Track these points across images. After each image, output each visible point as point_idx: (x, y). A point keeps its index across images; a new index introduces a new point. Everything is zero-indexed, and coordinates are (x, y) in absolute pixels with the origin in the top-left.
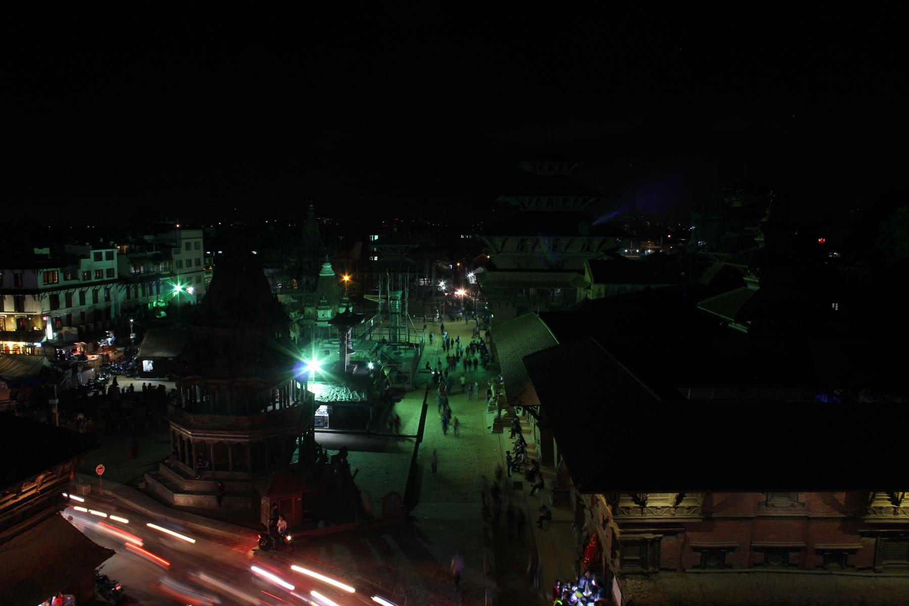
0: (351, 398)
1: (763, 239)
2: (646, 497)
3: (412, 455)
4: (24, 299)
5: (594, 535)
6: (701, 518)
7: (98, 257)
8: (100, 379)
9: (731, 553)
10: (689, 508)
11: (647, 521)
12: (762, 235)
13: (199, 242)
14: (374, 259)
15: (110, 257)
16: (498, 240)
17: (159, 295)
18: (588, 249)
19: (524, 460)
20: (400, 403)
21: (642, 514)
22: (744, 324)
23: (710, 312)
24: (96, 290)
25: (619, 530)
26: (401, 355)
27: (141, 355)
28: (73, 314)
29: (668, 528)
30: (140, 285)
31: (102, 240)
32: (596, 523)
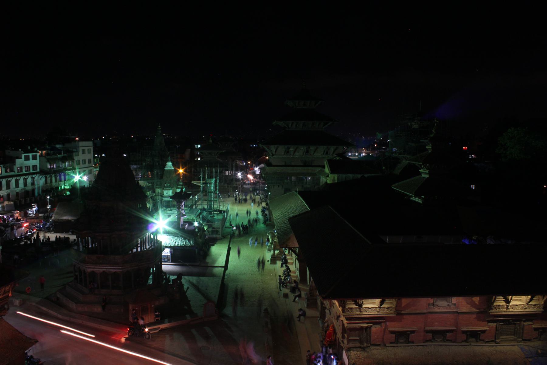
0: (184, 243)
1: (431, 147)
2: (362, 302)
3: (221, 278)
5: (331, 325)
6: (394, 314)
7: (27, 158)
8: (28, 233)
9: (413, 334)
10: (388, 308)
11: (363, 316)
13: (90, 149)
14: (198, 159)
15: (34, 158)
16: (273, 148)
17: (65, 182)
18: (327, 153)
19: (289, 280)
20: (214, 246)
21: (360, 312)
22: (420, 198)
23: (400, 190)
24: (26, 178)
25: (347, 322)
26: (214, 218)
27: (54, 218)
28: (11, 193)
29: (376, 320)
30: (53, 175)
31: (29, 148)
32: (333, 318)
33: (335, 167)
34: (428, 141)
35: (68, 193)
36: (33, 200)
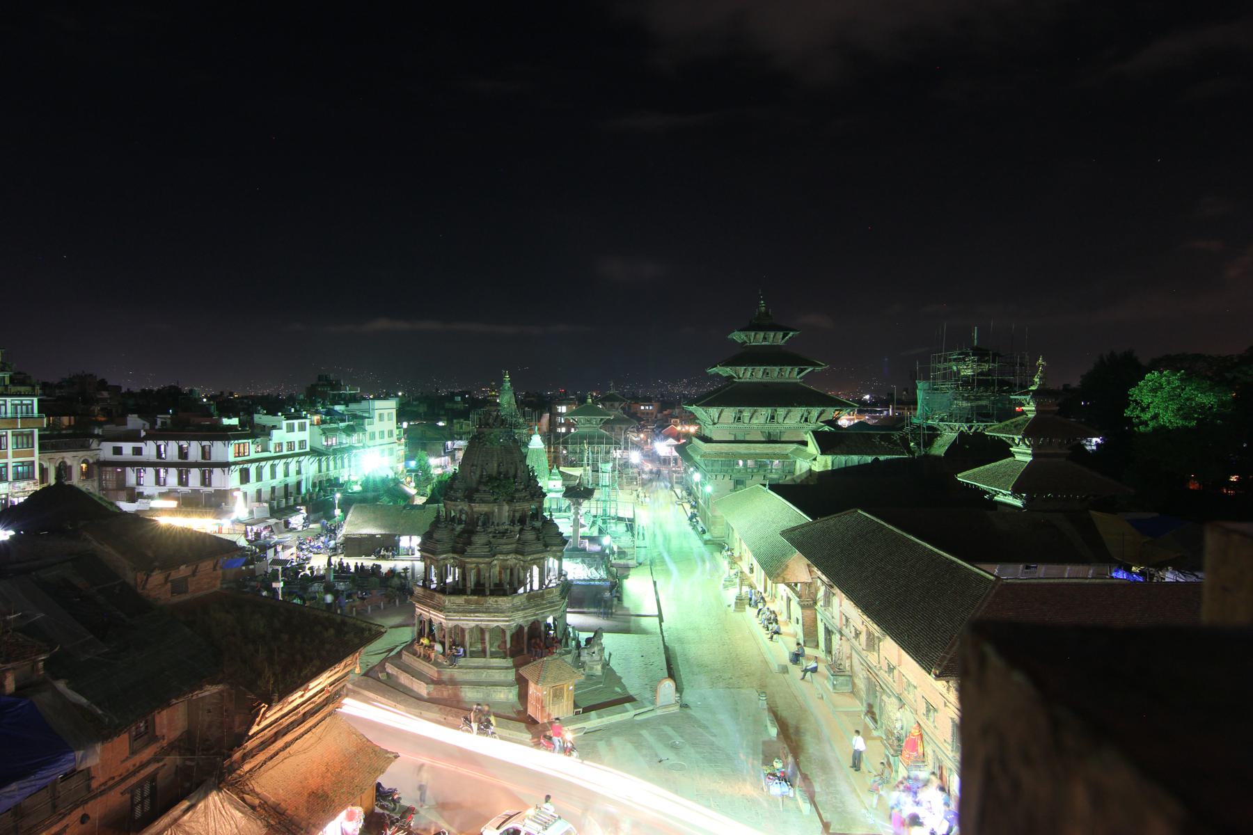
1: (1034, 408)
4: (211, 472)
7: (291, 429)
12: (1031, 404)
15: (302, 428)
16: (714, 411)
18: (806, 420)
20: (629, 579)
22: (1021, 498)
23: (976, 484)
30: (332, 457)
31: (293, 410)
33: (830, 441)
34: (1028, 398)
35: (357, 488)
36: (300, 500)
